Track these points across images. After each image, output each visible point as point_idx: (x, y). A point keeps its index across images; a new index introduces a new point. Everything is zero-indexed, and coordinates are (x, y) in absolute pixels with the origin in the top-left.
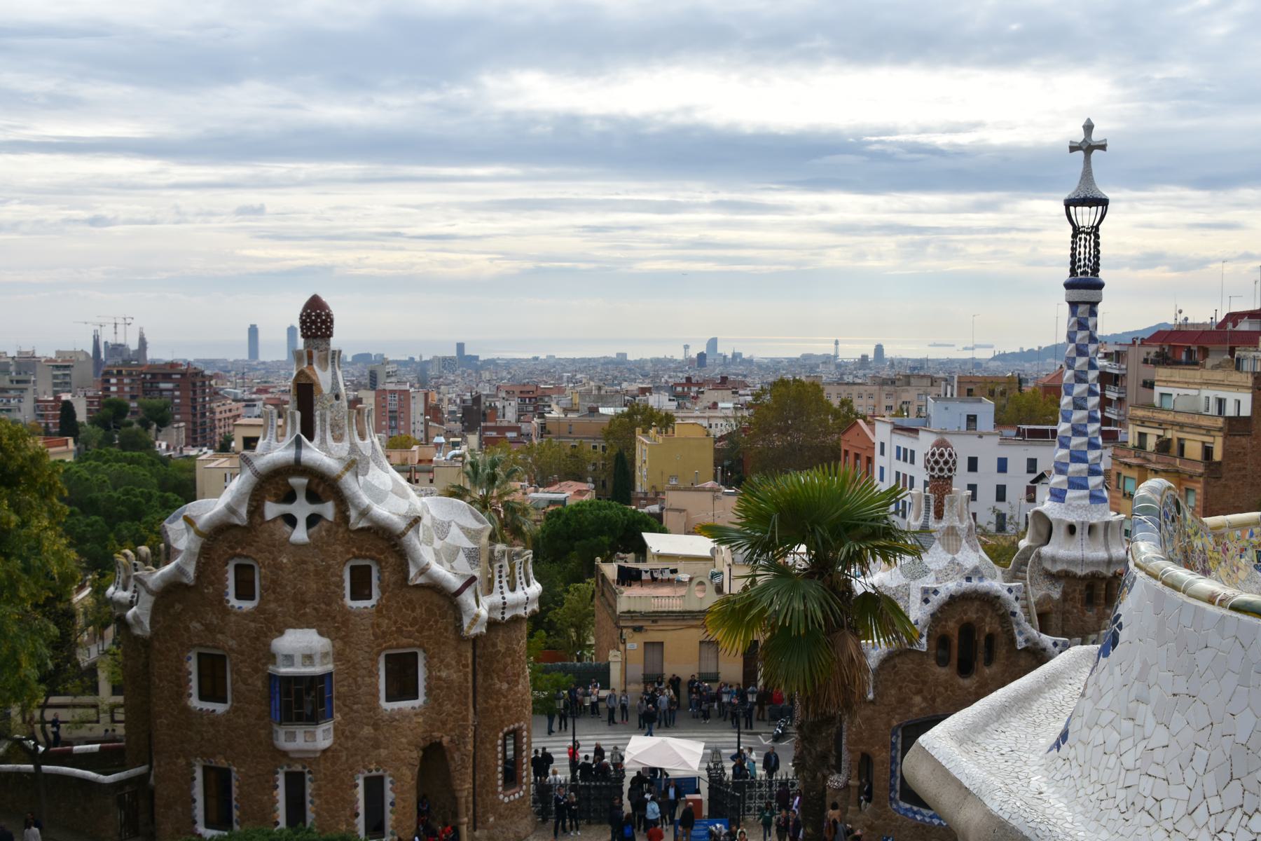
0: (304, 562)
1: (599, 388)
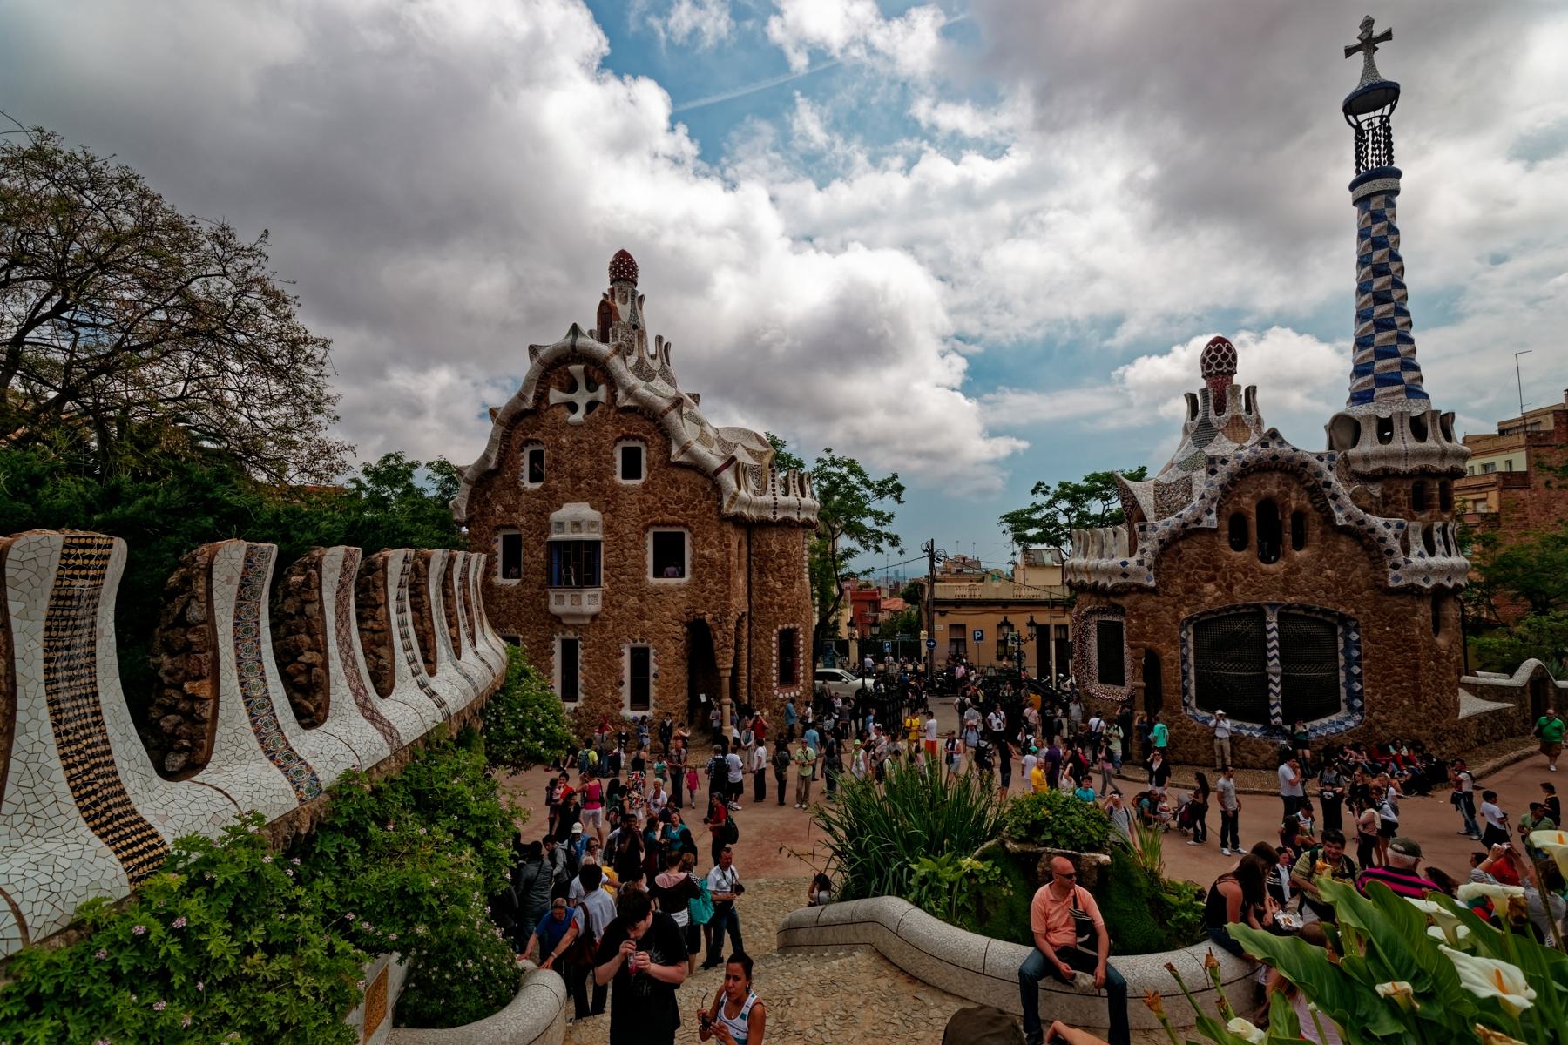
0: (580, 441)
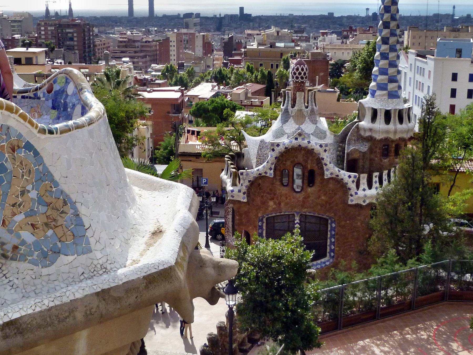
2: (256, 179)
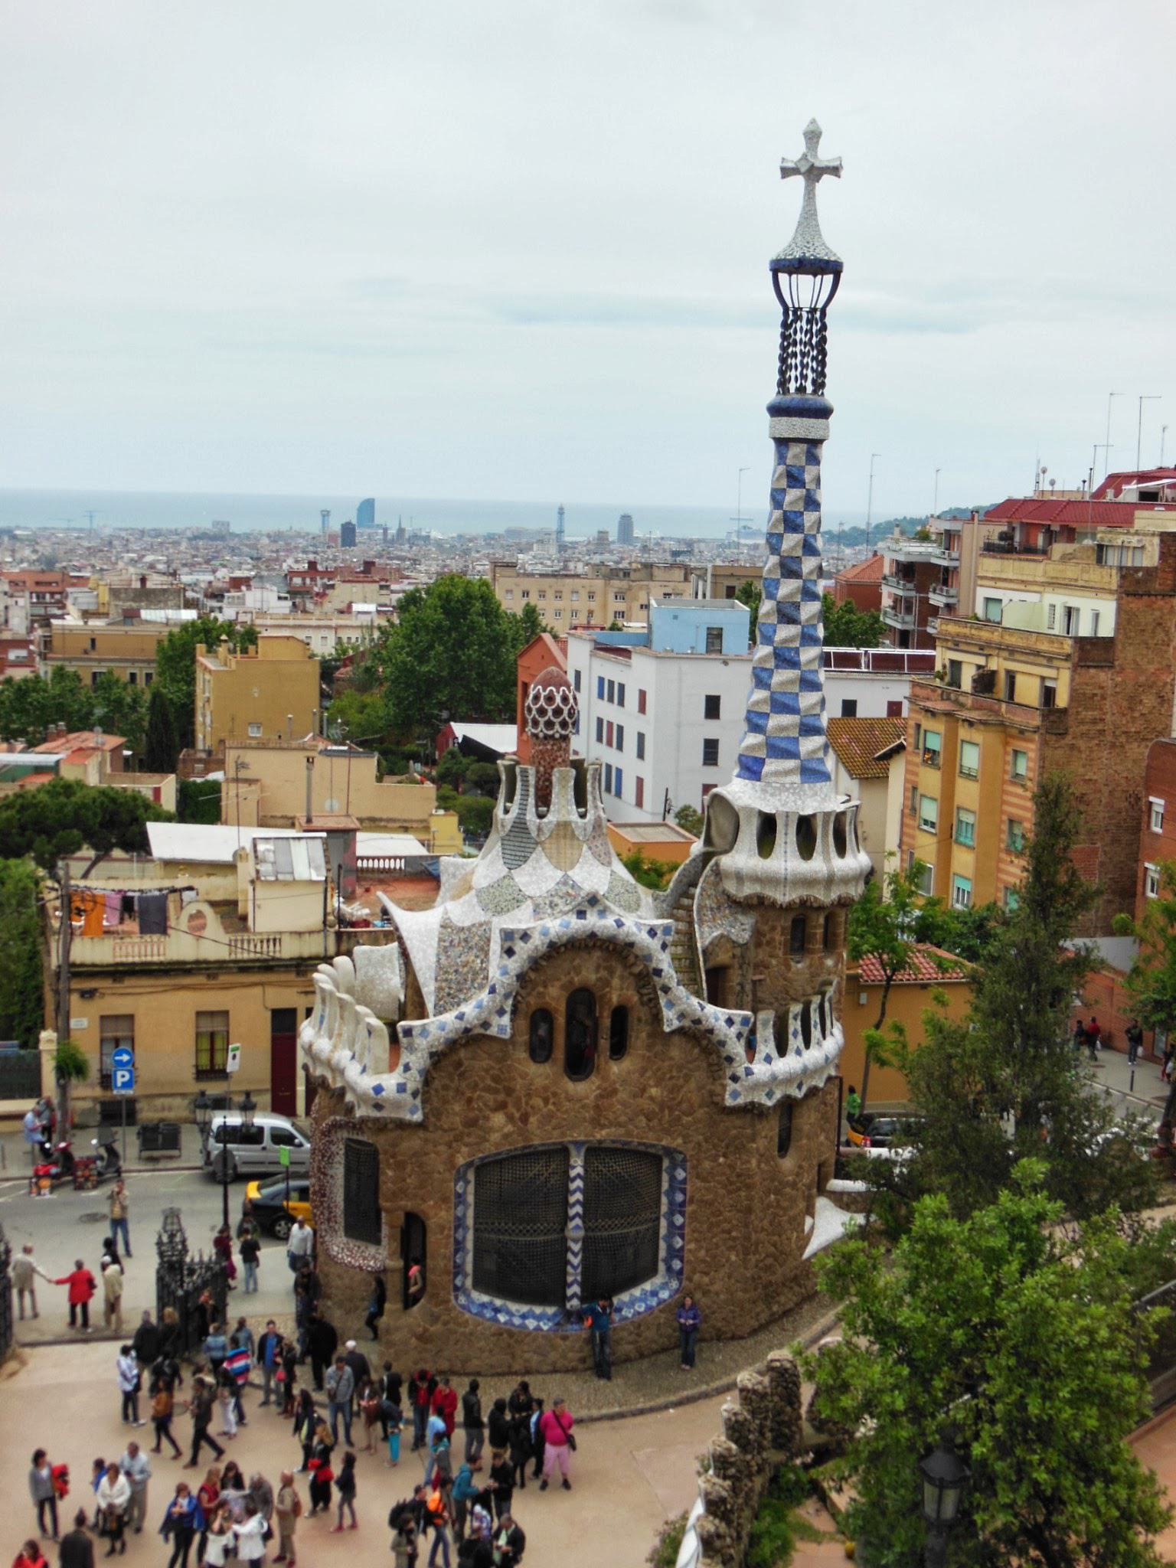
1: (143, 580)
2: (453, 1045)
